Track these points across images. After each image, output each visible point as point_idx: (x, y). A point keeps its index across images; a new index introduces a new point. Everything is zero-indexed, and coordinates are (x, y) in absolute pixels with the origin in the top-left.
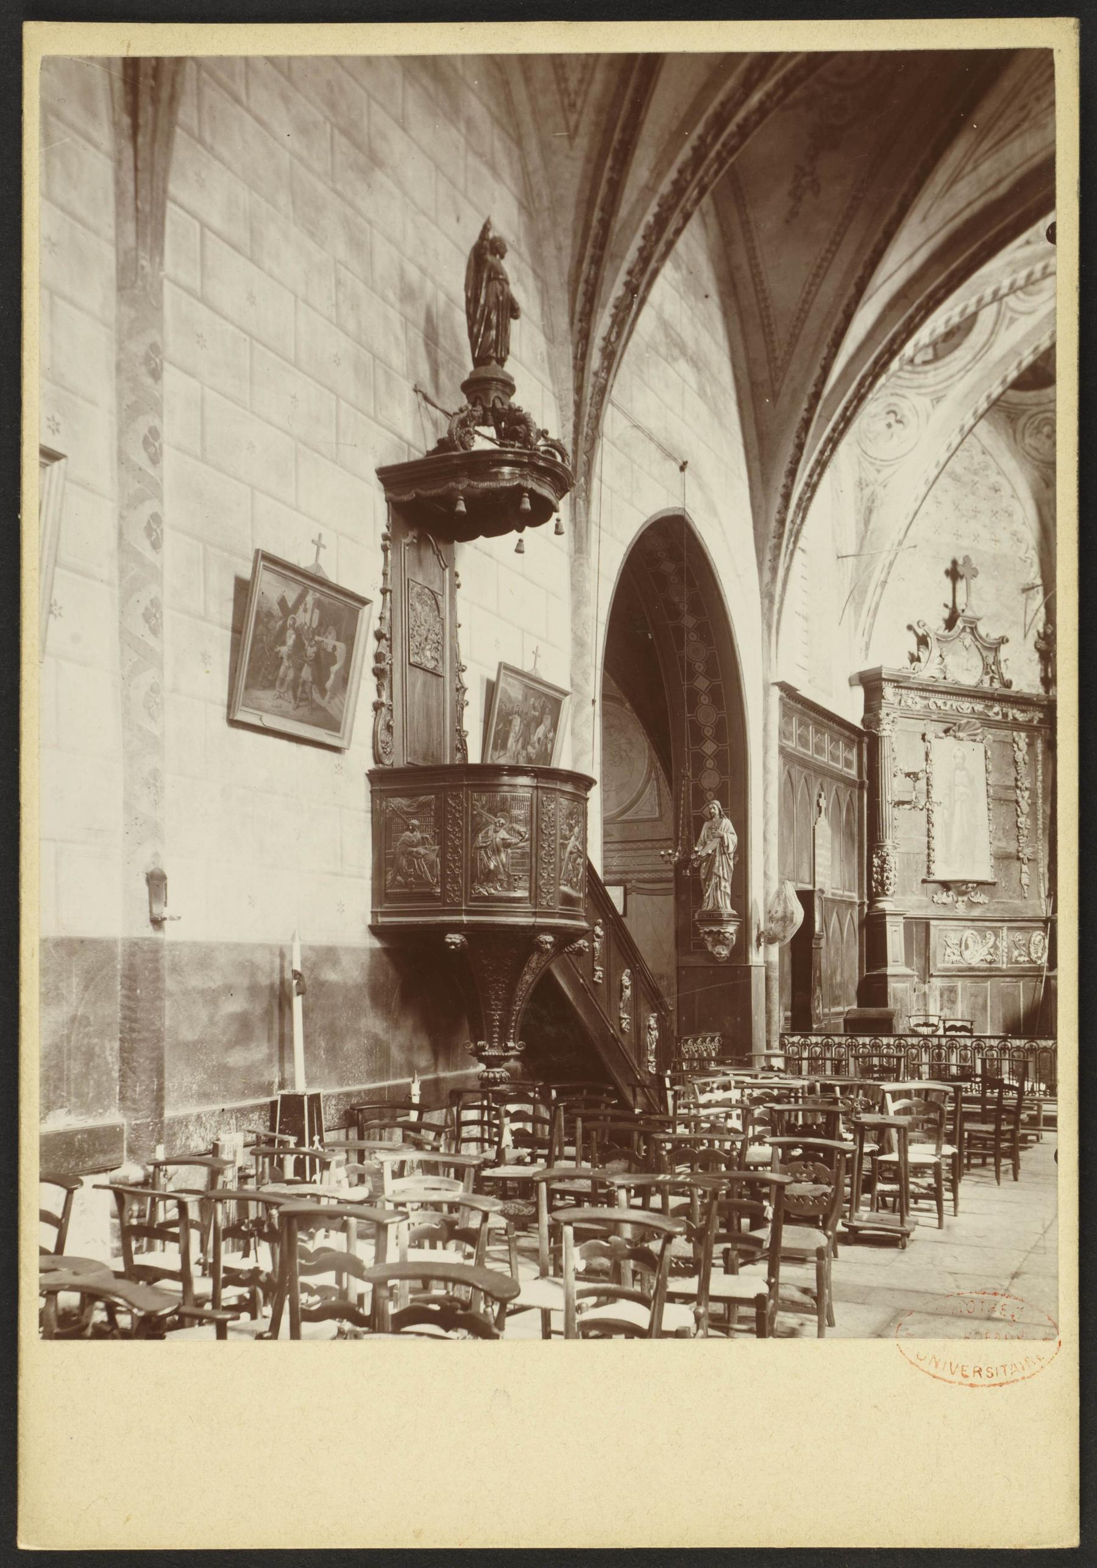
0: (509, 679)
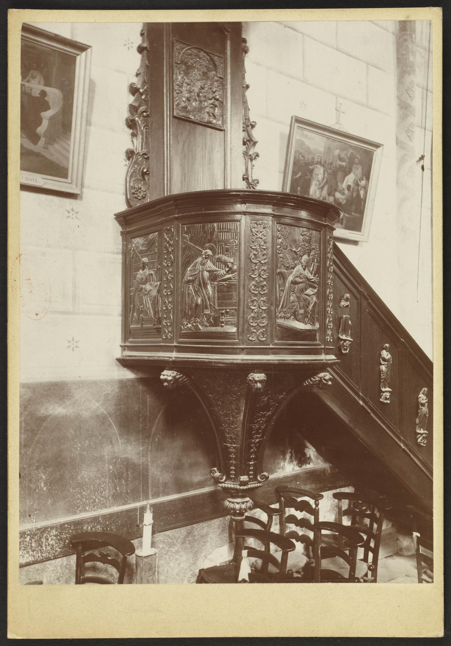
0: (306, 132)
